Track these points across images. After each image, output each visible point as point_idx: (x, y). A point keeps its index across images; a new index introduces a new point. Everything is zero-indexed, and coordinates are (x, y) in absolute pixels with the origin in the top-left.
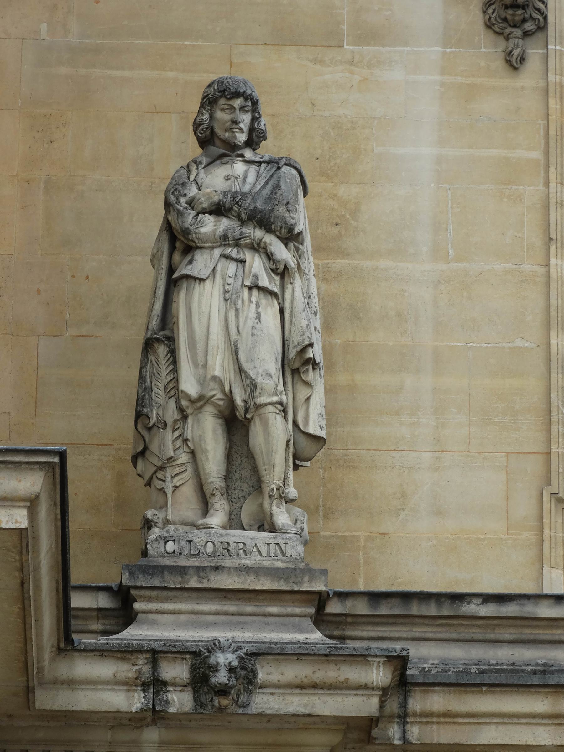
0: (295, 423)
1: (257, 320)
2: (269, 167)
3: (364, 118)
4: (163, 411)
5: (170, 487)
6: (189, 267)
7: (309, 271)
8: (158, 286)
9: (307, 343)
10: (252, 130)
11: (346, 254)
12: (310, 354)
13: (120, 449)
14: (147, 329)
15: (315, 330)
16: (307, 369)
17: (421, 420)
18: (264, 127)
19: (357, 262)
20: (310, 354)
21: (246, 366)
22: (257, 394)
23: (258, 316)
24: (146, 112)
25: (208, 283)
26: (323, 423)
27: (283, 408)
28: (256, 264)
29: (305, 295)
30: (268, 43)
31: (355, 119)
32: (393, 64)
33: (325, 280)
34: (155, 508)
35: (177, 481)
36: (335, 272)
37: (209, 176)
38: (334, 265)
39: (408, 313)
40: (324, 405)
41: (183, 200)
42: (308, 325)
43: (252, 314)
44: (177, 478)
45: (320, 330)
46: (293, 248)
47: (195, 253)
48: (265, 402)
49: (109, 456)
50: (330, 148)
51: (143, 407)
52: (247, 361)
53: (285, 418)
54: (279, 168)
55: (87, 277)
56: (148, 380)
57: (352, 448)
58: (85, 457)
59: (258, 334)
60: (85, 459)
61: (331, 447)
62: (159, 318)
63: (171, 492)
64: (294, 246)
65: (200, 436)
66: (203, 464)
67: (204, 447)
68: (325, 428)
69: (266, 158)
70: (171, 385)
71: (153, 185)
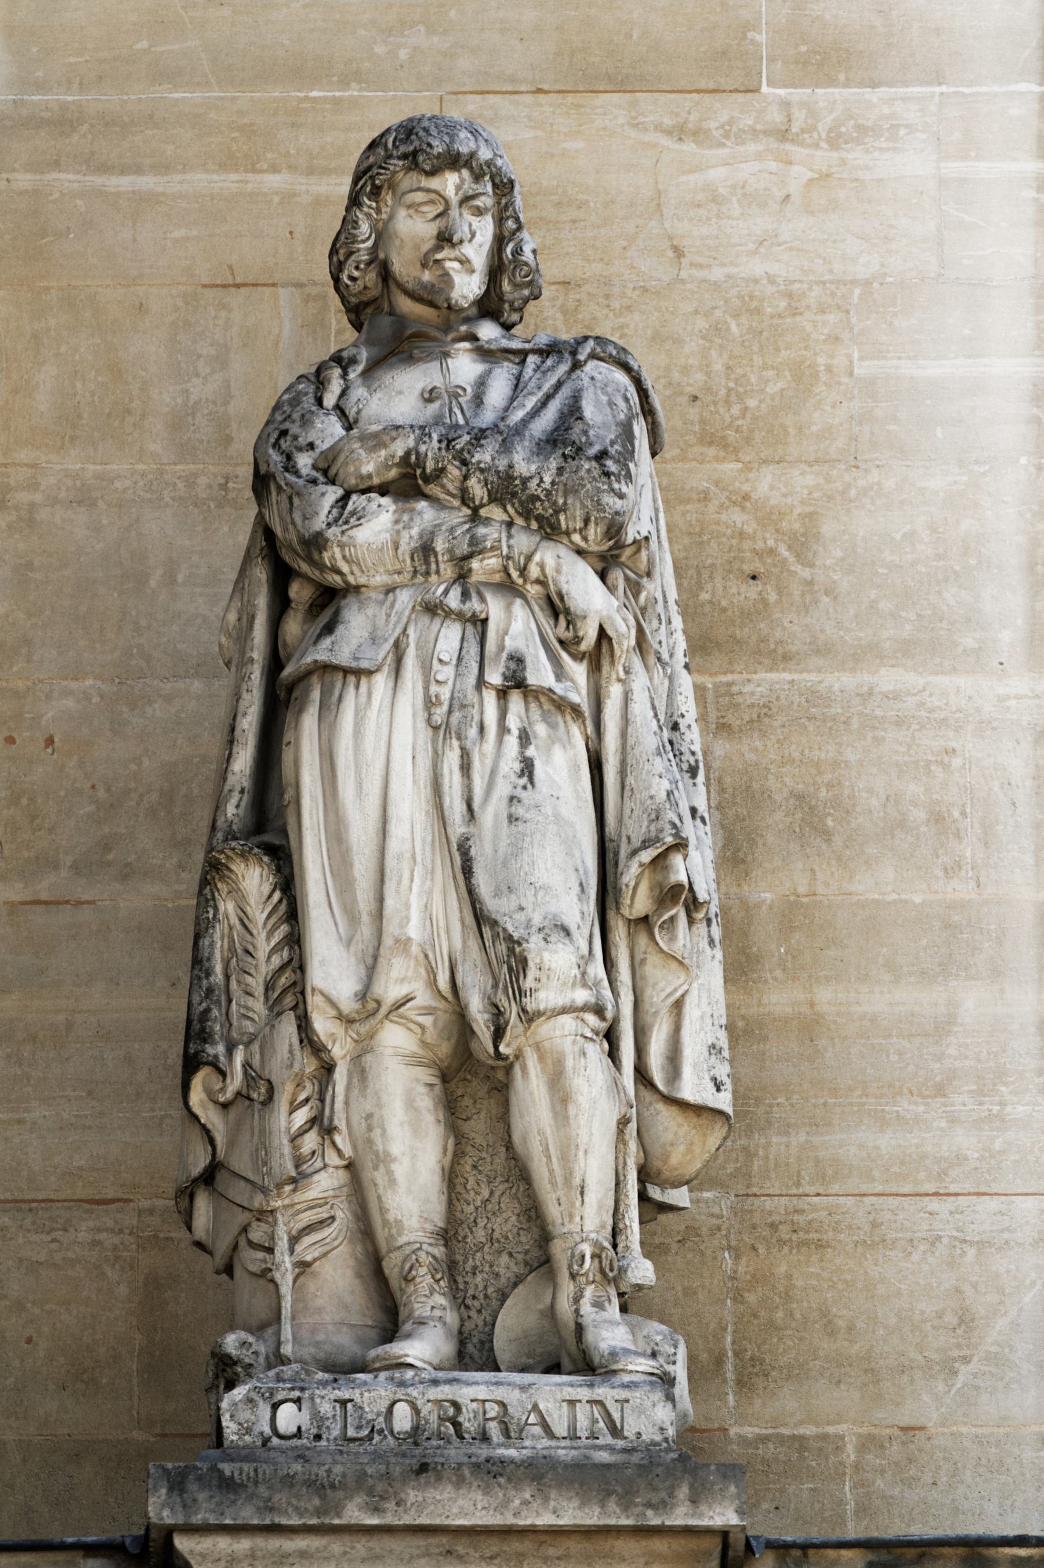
0: (642, 1074)
1: (524, 780)
2: (549, 362)
3: (824, 283)
4: (262, 1054)
5: (289, 1265)
6: (327, 642)
7: (671, 656)
8: (242, 708)
9: (669, 840)
10: (495, 271)
11: (783, 659)
12: (679, 871)
13: (151, 1211)
14: (213, 828)
15: (694, 817)
16: (672, 919)
17: (1009, 1109)
18: (531, 256)
19: (813, 677)
20: (679, 871)
21: (492, 904)
22: (528, 983)
23: (527, 768)
24: (205, 286)
25: (381, 682)
26: (723, 1071)
27: (604, 1025)
28: (517, 626)
29: (662, 717)
30: (546, 87)
31: (797, 285)
32: (902, 132)
33: (723, 728)
34: (248, 1329)
35: (307, 1248)
36: (752, 706)
37: (379, 395)
38: (747, 689)
39: (964, 814)
40: (724, 1021)
41: (304, 461)
42: (669, 794)
43: (510, 763)
44: (307, 1240)
45: (706, 816)
46: (621, 584)
47: (343, 603)
48: (551, 1004)
49: (121, 1231)
50: (728, 368)
51: (205, 1041)
52: (497, 894)
53: (613, 1054)
54: (576, 366)
55: (50, 741)
56: (218, 969)
57: (812, 1190)
58: (54, 1235)
59: (528, 816)
60: (53, 1241)
61: (755, 1190)
62: (246, 797)
63: (290, 1278)
64: (627, 579)
65: (369, 1116)
66: (379, 1197)
67: (380, 1148)
68: (728, 1085)
69: (542, 340)
70: (283, 981)
71: (231, 485)
